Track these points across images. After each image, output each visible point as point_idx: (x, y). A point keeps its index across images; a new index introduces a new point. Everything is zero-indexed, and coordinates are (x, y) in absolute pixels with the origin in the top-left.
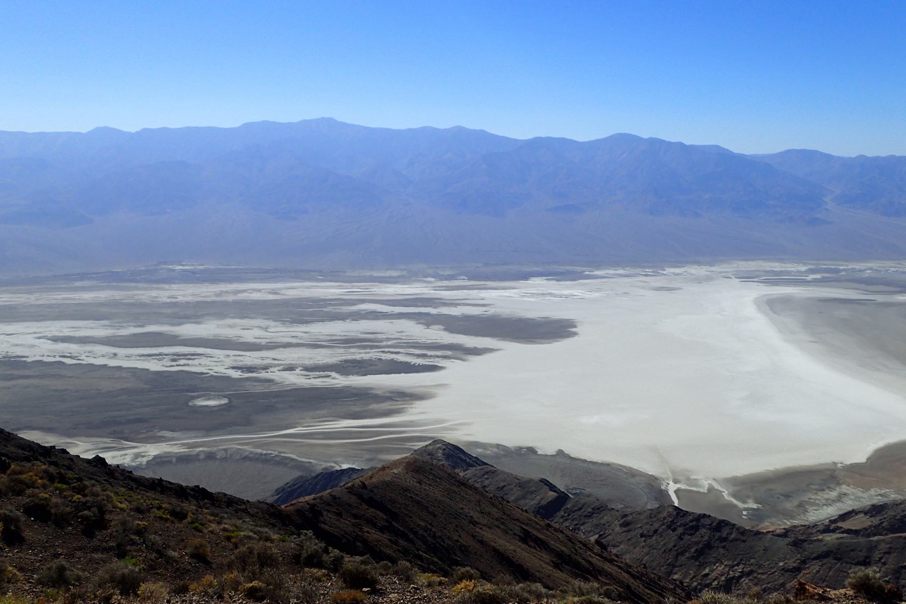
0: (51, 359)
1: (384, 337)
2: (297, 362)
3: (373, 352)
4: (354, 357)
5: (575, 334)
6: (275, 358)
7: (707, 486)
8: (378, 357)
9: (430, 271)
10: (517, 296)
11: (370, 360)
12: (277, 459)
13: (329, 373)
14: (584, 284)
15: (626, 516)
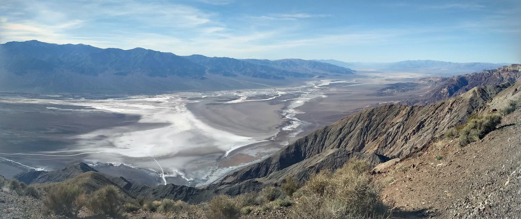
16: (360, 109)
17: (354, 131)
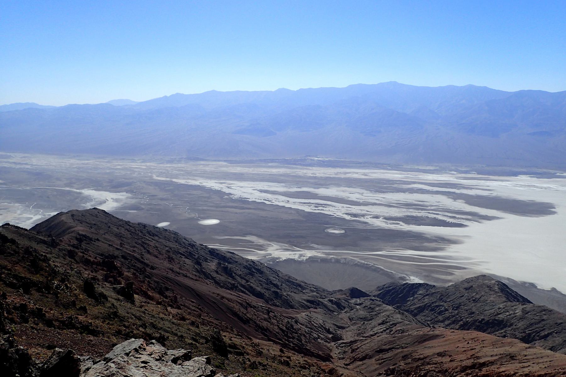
0: (260, 201)
1: (429, 204)
2: (380, 214)
3: (423, 212)
4: (412, 214)
5: (554, 213)
6: (368, 210)
8: (426, 216)
9: (453, 168)
10: (510, 186)
11: (422, 217)
12: (373, 268)
13: (398, 222)
14: (558, 181)
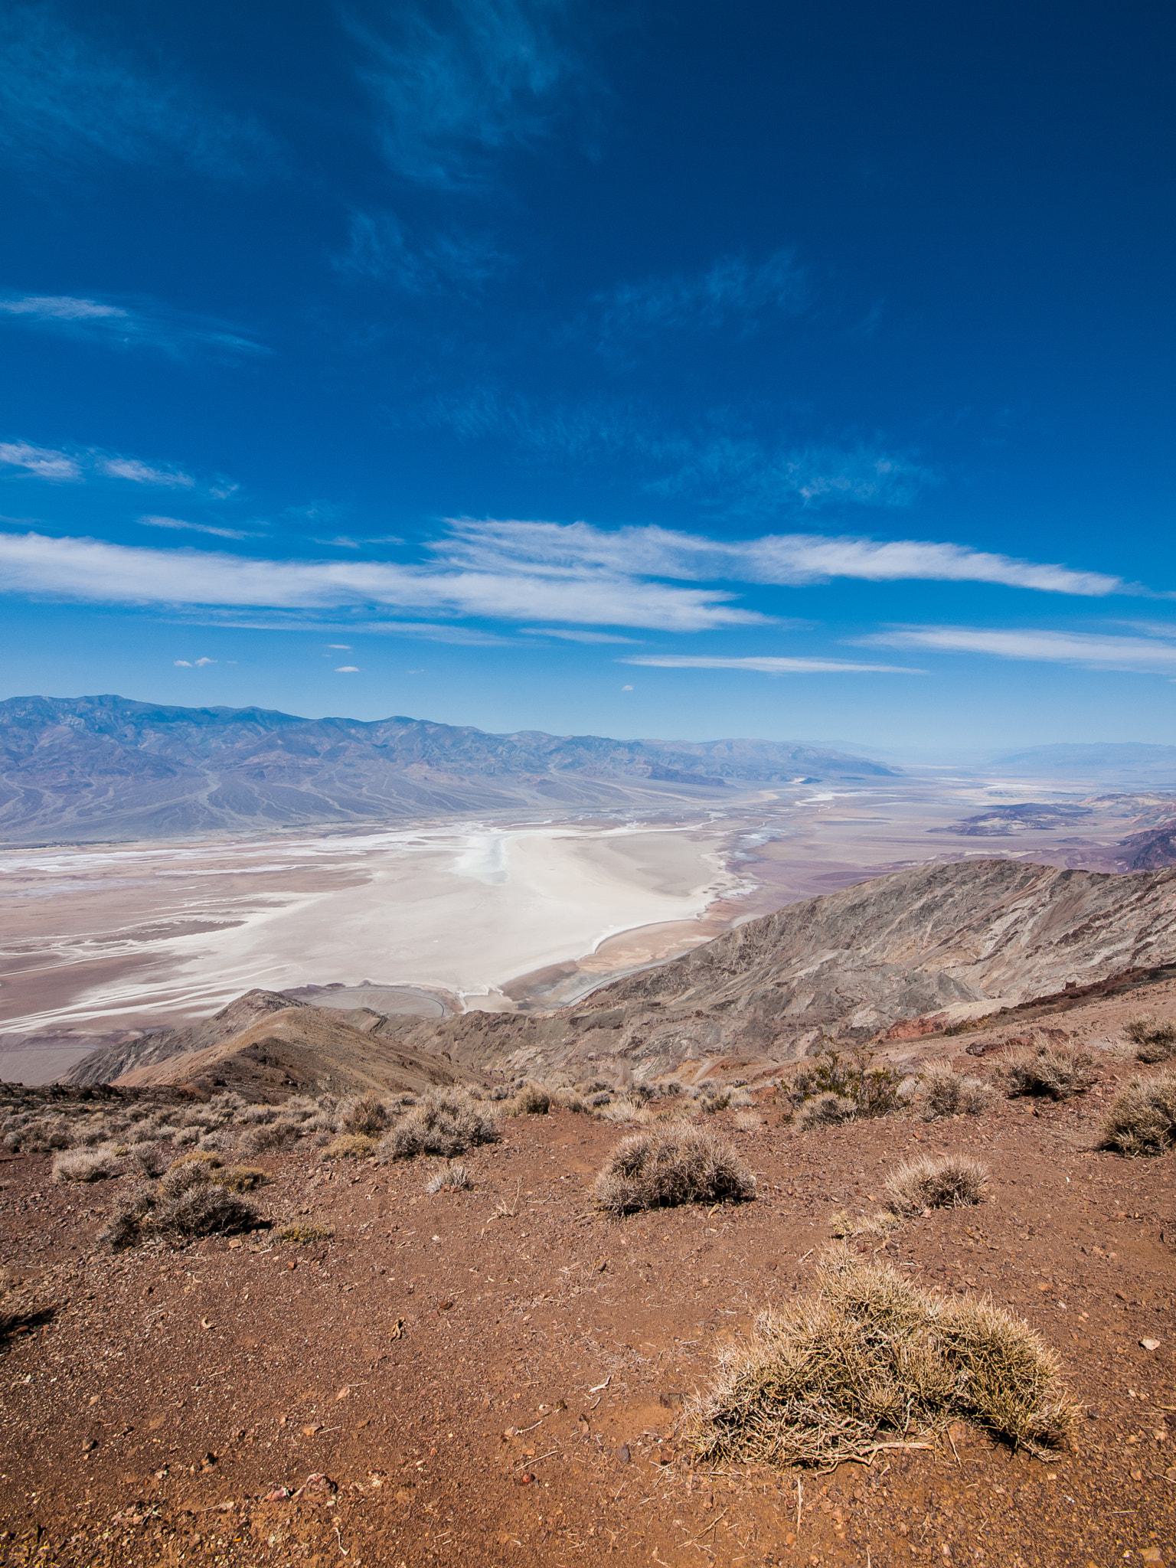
7: (488, 990)
15: (440, 1026)
16: (912, 862)
17: (891, 916)
